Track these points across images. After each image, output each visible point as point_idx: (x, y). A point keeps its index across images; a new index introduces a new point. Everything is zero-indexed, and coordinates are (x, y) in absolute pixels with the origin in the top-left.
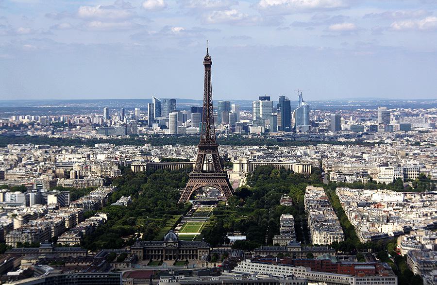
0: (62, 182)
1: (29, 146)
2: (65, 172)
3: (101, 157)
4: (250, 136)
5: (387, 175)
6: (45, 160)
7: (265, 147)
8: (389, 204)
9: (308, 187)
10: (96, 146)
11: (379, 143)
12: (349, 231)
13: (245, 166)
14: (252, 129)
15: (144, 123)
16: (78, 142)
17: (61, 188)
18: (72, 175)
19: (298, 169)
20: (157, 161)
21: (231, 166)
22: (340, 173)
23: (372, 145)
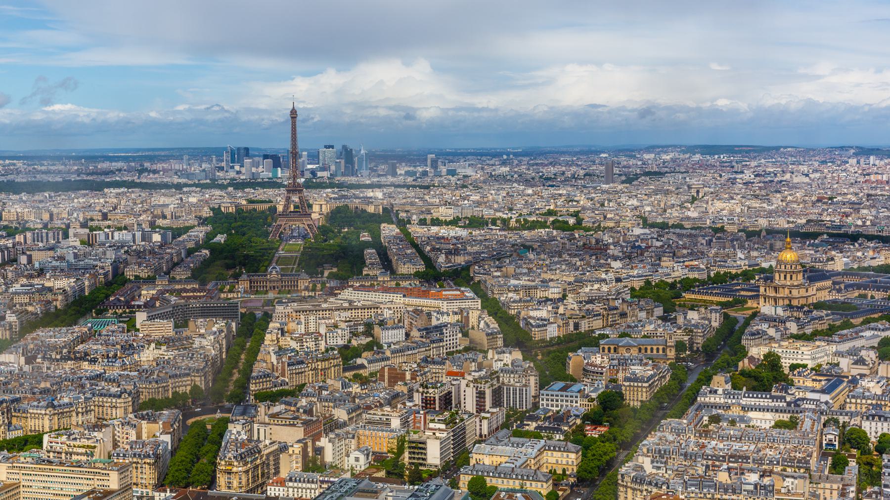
0: (160, 222)
1: (122, 190)
2: (162, 212)
3: (193, 200)
4: (318, 180)
6: (142, 203)
7: (336, 190)
9: (383, 225)
10: (185, 189)
11: (434, 186)
12: (429, 262)
13: (324, 206)
14: (319, 174)
15: (221, 169)
16: (166, 186)
17: (159, 227)
18: (169, 217)
19: (371, 209)
20: (244, 202)
21: (310, 206)
22: (407, 211)
23: (427, 187)
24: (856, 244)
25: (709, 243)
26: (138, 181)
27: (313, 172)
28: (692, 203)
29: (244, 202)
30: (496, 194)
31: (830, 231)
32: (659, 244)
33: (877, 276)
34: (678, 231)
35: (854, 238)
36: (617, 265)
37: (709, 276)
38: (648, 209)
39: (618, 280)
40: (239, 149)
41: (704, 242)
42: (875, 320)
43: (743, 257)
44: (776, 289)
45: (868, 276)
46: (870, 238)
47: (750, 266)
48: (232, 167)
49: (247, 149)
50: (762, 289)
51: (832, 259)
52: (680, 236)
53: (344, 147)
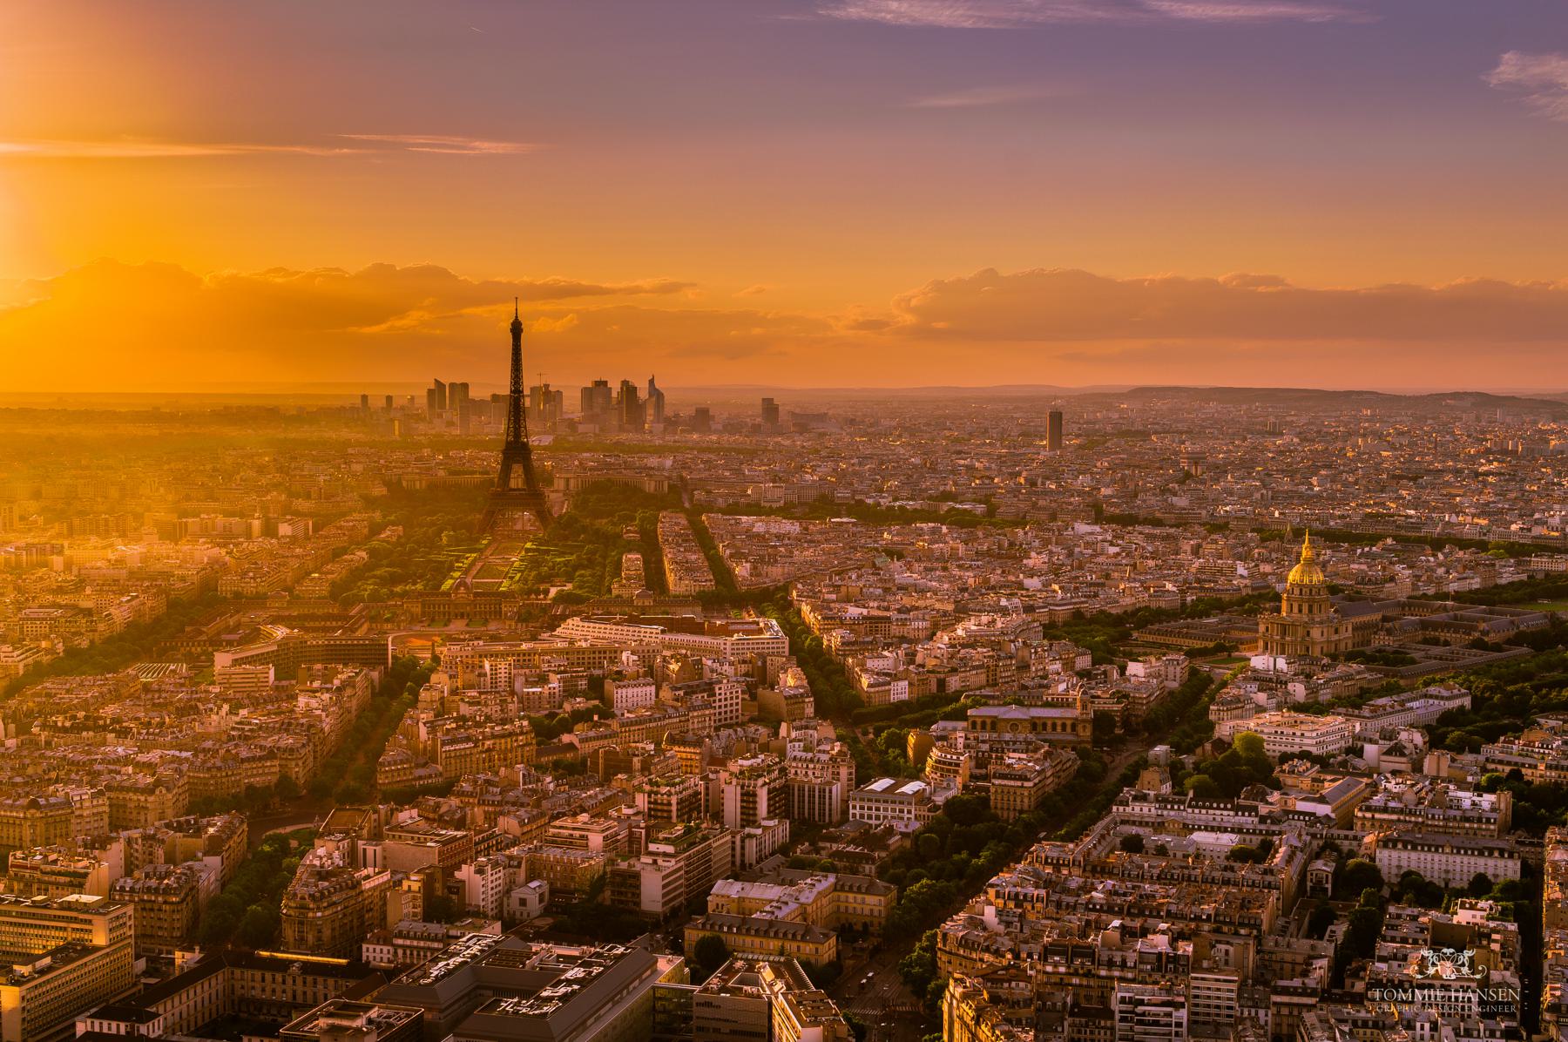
0: (302, 504)
5: (774, 493)
8: (779, 537)
13: (572, 482)
14: (581, 428)
19: (650, 486)
20: (442, 473)
21: (550, 482)
22: (709, 492)
24: (1441, 556)
25: (1196, 551)
26: (282, 436)
27: (572, 424)
28: (1182, 482)
29: (442, 473)
30: (860, 464)
31: (1403, 532)
32: (1113, 550)
33: (1460, 609)
34: (1148, 530)
35: (1437, 544)
36: (1033, 583)
37: (1184, 604)
38: (1105, 491)
39: (1029, 609)
40: (452, 385)
41: (1188, 549)
43: (1245, 573)
44: (1284, 629)
45: (1445, 609)
46: (1463, 544)
47: (1254, 589)
48: (440, 416)
49: (465, 386)
50: (1262, 628)
51: (1392, 579)
52: (1150, 538)
53: (625, 383)
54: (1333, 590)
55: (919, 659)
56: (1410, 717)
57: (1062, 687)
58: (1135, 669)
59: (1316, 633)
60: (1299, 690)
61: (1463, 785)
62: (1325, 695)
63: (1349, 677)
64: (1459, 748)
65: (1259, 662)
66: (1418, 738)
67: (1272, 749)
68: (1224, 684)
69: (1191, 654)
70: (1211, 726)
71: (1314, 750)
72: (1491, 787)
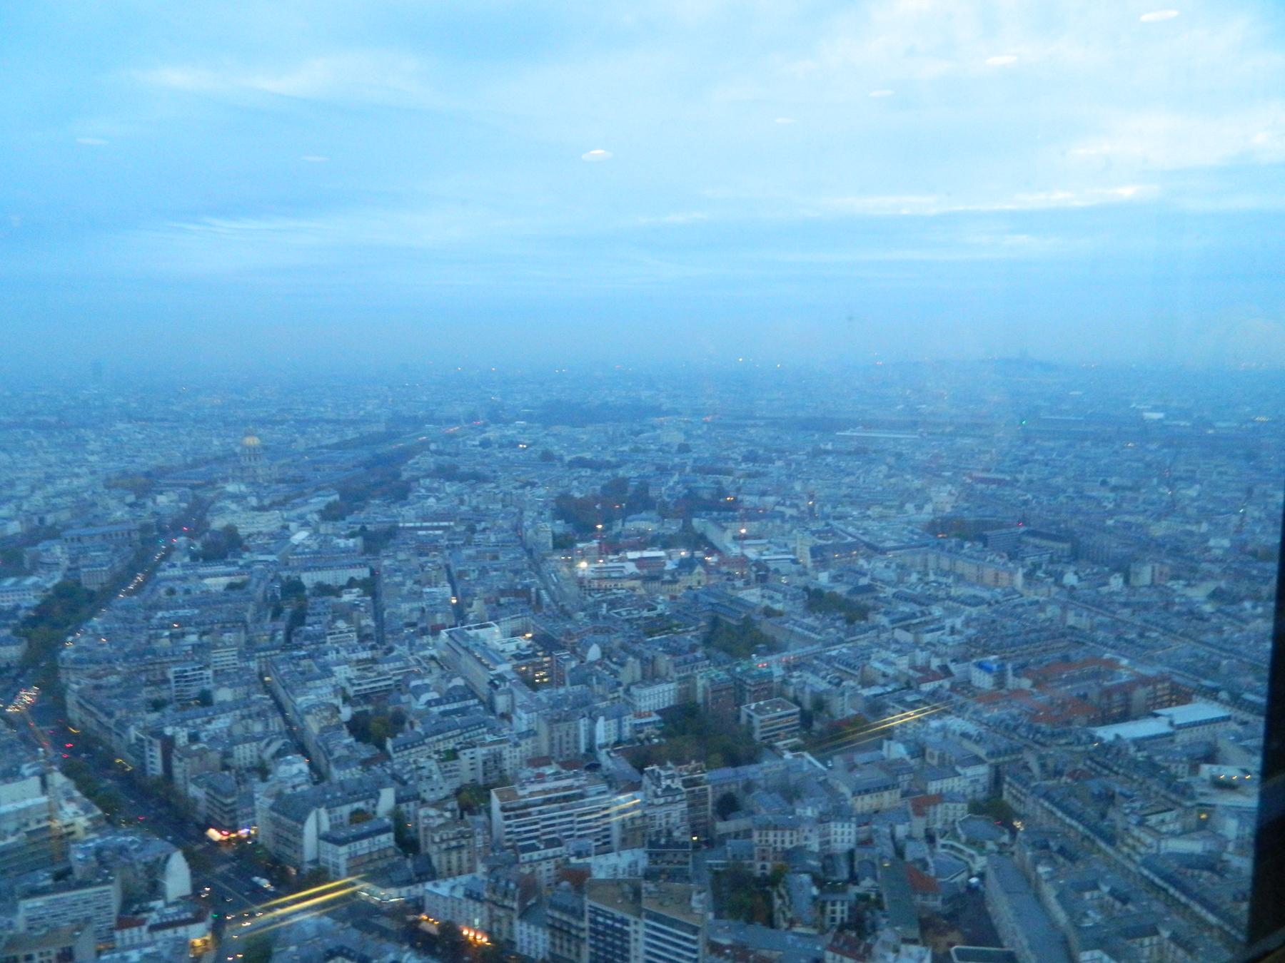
36: (92, 458)
39: (93, 473)
42: (323, 488)
54: (266, 448)
55: (25, 507)
56: (312, 507)
57: (119, 514)
58: (162, 499)
59: (260, 471)
60: (253, 501)
61: (339, 536)
62: (266, 502)
63: (277, 491)
64: (335, 519)
65: (231, 488)
66: (316, 517)
67: (242, 532)
68: (213, 502)
69: (193, 487)
70: (208, 524)
71: (265, 530)
72: (352, 535)
